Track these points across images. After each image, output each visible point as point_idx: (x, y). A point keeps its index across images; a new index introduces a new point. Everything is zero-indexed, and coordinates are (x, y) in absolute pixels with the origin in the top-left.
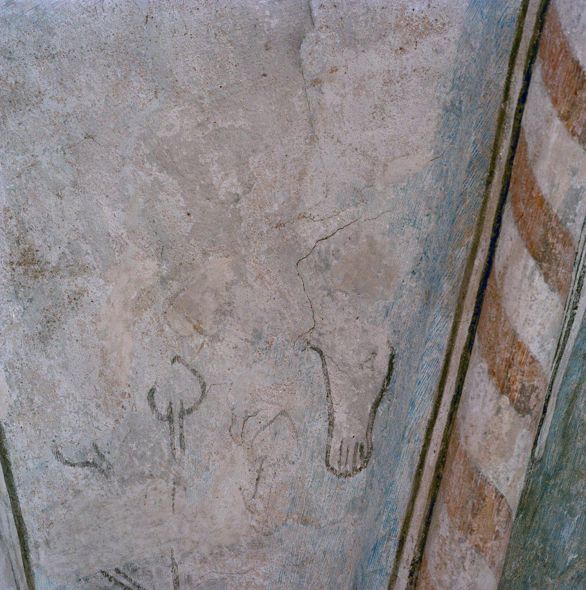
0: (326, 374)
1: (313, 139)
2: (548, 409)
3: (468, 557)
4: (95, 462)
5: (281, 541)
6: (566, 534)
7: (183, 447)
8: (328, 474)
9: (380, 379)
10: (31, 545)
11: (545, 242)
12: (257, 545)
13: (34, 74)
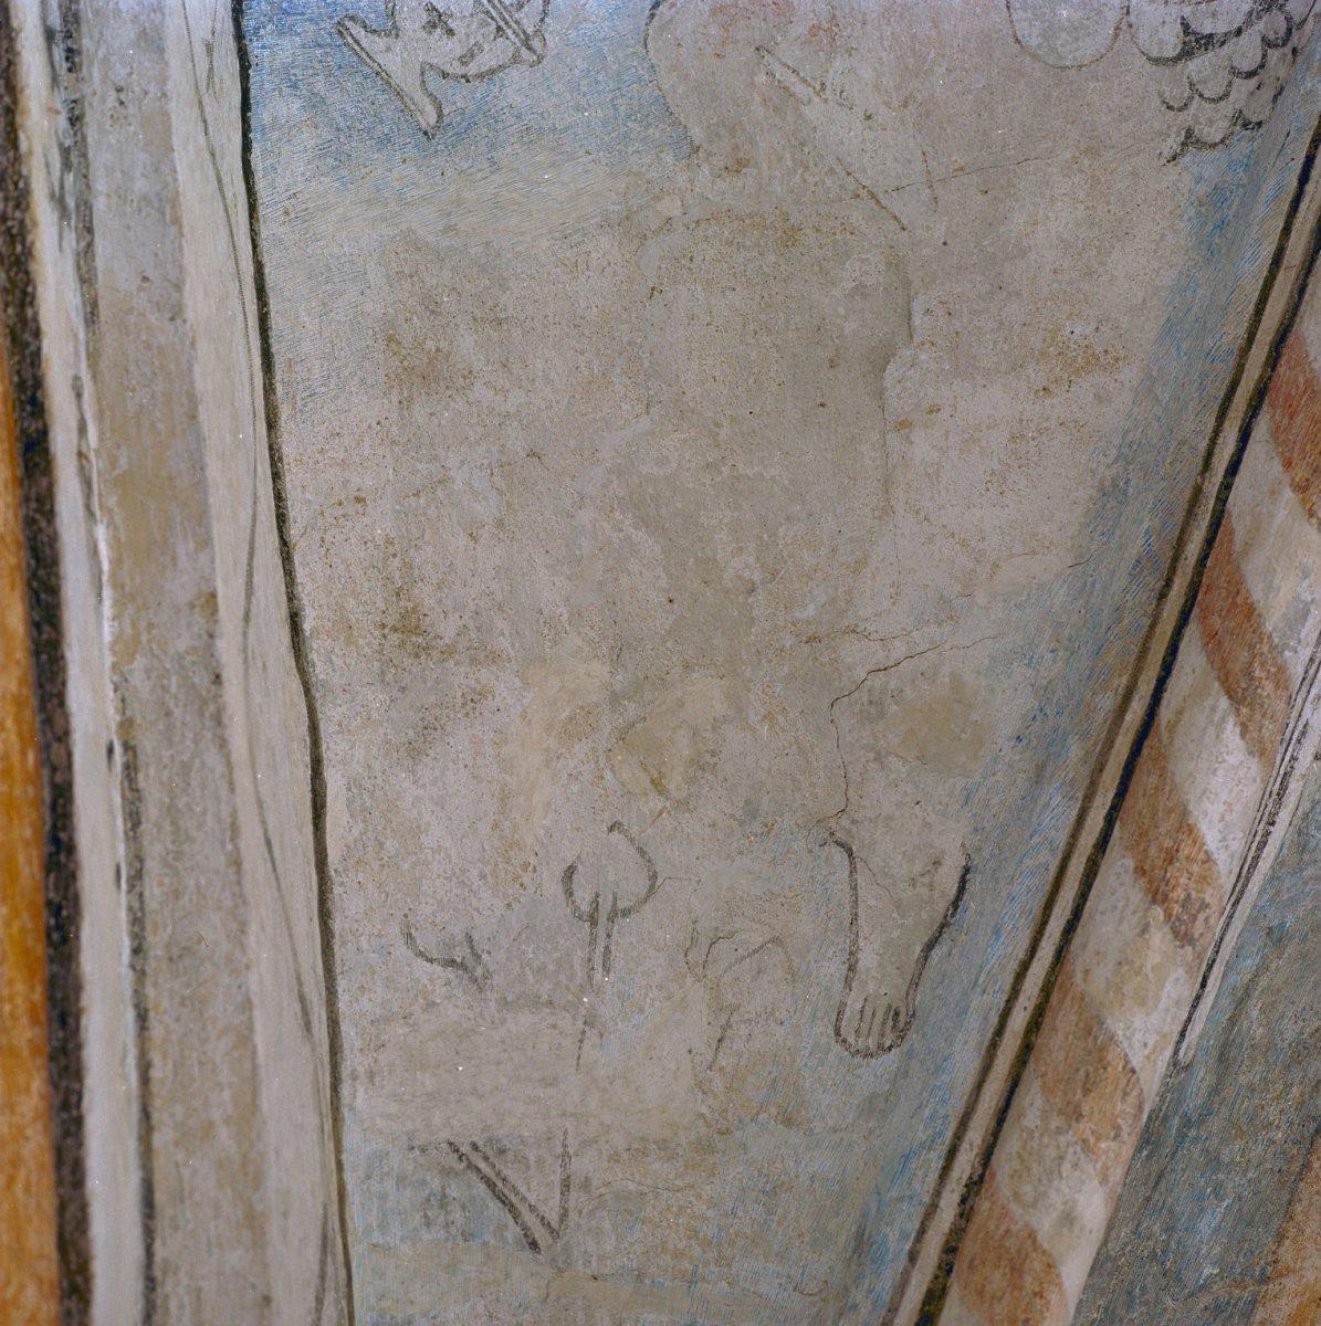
0: (854, 888)
1: (886, 511)
2: (1210, 982)
3: (1069, 1156)
4: (464, 963)
5: (743, 1146)
6: (1206, 1226)
7: (607, 969)
8: (837, 1048)
9: (942, 905)
10: (345, 1072)
11: (1249, 674)
12: (704, 1147)
13: (466, 345)
